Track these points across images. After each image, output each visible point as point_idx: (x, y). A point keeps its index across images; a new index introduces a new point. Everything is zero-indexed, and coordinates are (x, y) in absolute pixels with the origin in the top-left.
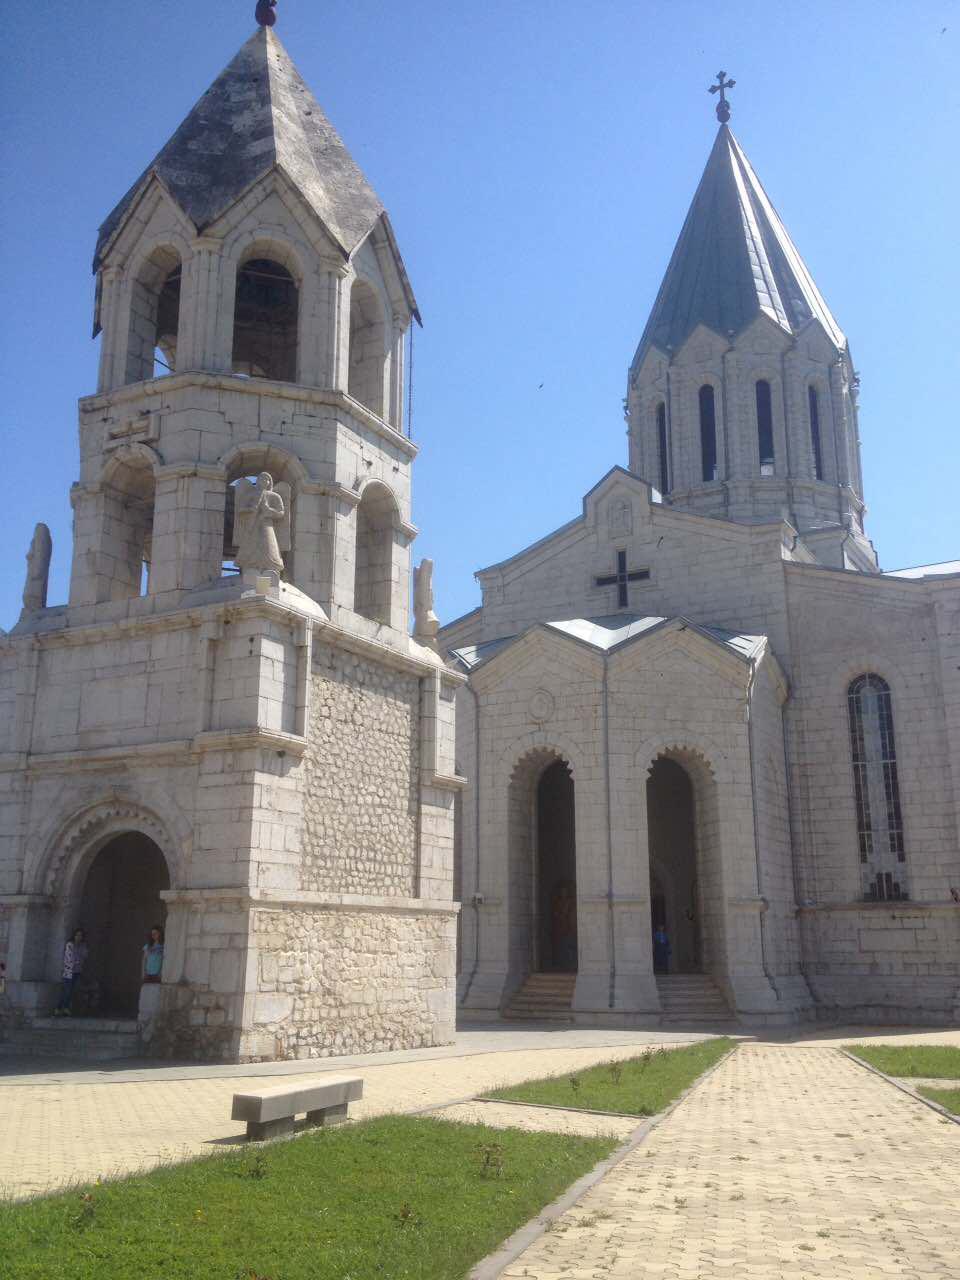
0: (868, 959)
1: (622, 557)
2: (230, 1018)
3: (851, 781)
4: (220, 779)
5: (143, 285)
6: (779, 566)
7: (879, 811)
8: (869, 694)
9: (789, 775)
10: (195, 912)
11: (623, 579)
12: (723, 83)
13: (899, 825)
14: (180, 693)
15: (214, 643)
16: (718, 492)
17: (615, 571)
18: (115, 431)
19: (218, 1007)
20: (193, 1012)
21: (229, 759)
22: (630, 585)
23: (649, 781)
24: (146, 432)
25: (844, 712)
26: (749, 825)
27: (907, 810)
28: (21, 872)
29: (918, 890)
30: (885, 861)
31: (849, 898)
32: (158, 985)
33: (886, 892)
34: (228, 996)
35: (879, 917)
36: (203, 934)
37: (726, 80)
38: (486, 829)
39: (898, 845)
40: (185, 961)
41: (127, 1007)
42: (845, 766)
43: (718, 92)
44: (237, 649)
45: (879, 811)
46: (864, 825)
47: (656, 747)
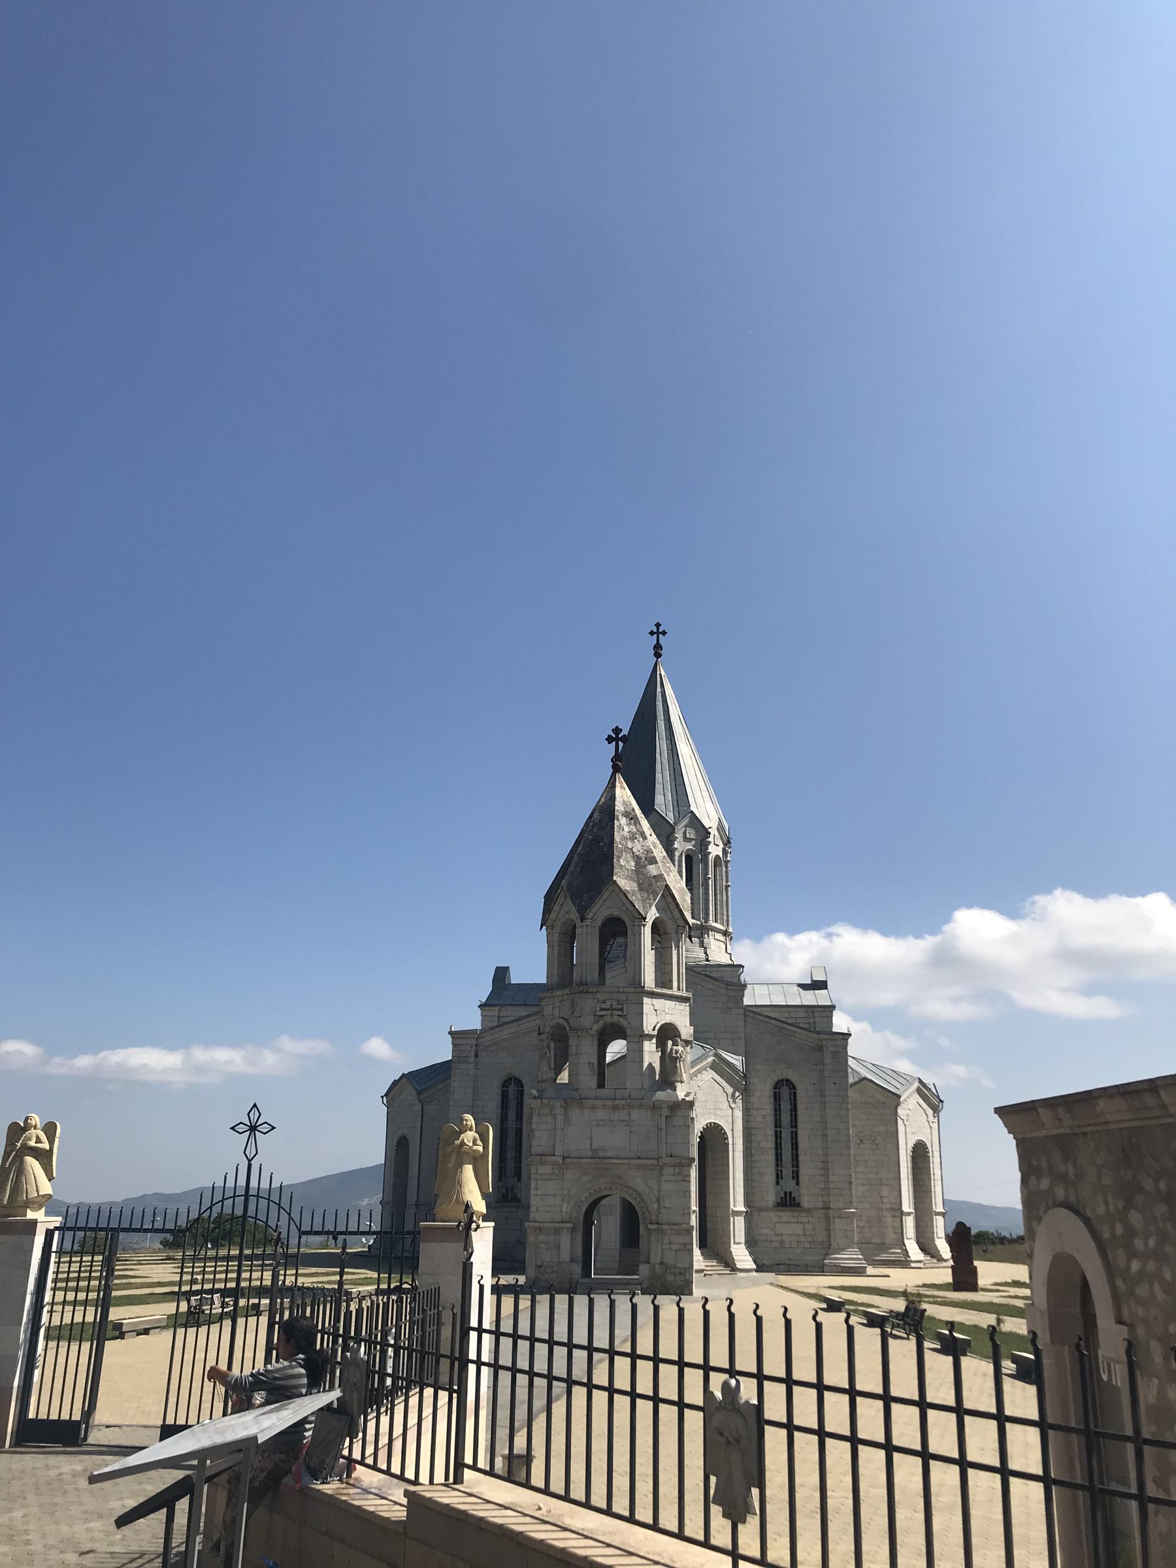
0: (778, 1238)
6: (742, 1011)
8: (785, 1091)
13: (797, 1166)
18: (604, 1006)
21: (677, 1169)
24: (622, 1010)
27: (801, 1158)
29: (805, 1202)
30: (788, 1184)
31: (771, 1205)
33: (788, 1202)
35: (786, 1215)
36: (670, 1243)
39: (796, 1176)
42: (770, 1132)
44: (677, 1121)
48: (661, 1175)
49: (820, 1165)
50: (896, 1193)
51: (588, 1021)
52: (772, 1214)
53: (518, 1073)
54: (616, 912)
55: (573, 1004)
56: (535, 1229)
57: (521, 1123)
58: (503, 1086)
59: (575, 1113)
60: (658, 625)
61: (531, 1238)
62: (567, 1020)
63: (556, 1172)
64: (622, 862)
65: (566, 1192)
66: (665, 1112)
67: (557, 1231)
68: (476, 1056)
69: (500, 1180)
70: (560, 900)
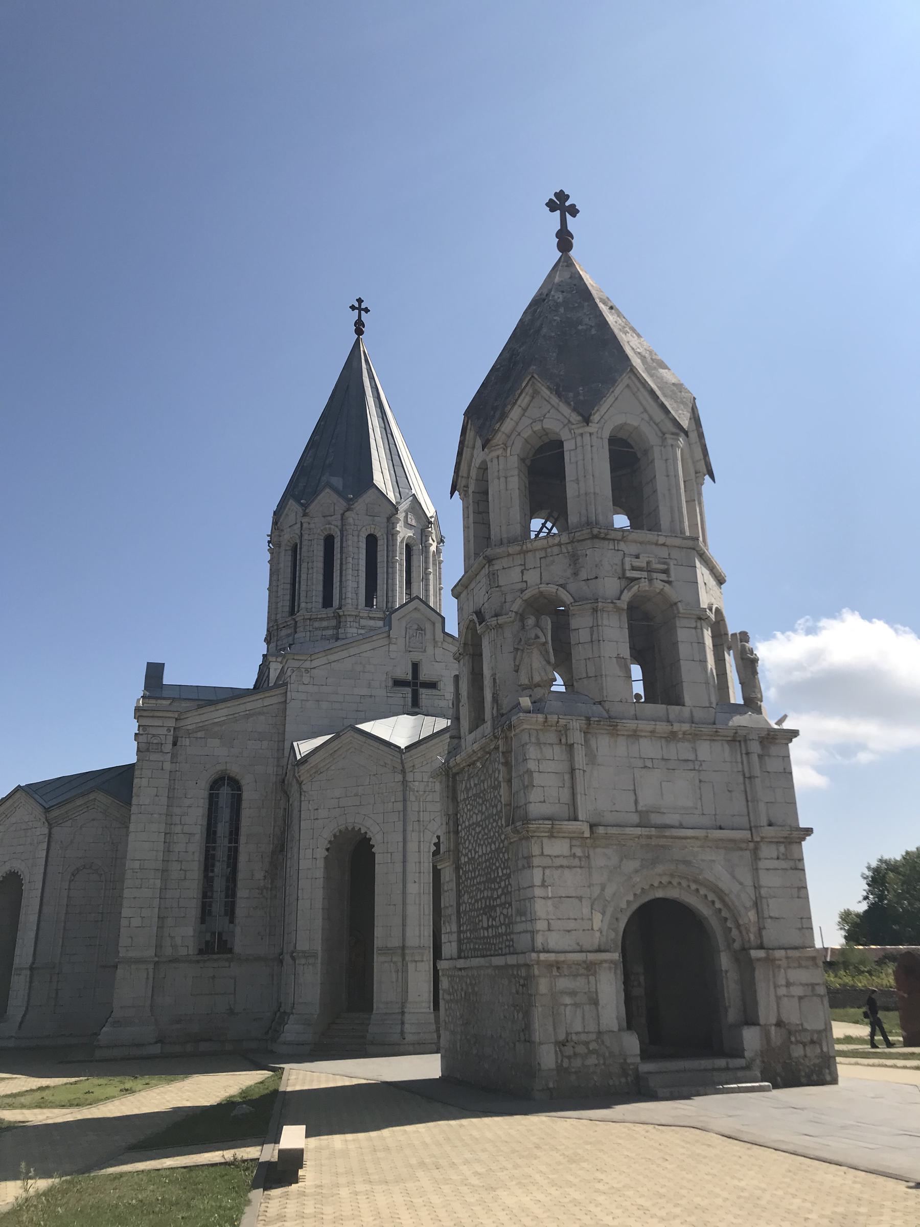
1: (415, 667)
2: (825, 1049)
4: (776, 864)
10: (779, 967)
11: (415, 684)
12: (359, 307)
14: (729, 791)
16: (379, 619)
17: (410, 677)
18: (637, 563)
19: (812, 1042)
20: (793, 1046)
21: (782, 849)
24: (666, 572)
28: (592, 929)
32: (758, 1027)
34: (819, 1032)
36: (788, 985)
37: (363, 306)
40: (778, 1007)
43: (357, 311)
44: (773, 765)
48: (756, 857)
51: (610, 585)
53: (234, 770)
55: (574, 559)
56: (550, 965)
57: (237, 841)
58: (212, 788)
59: (603, 744)
60: (360, 301)
61: (543, 985)
62: (561, 586)
63: (578, 852)
65: (597, 891)
66: (755, 747)
67: (590, 968)
68: (175, 744)
69: (203, 921)
70: (524, 400)
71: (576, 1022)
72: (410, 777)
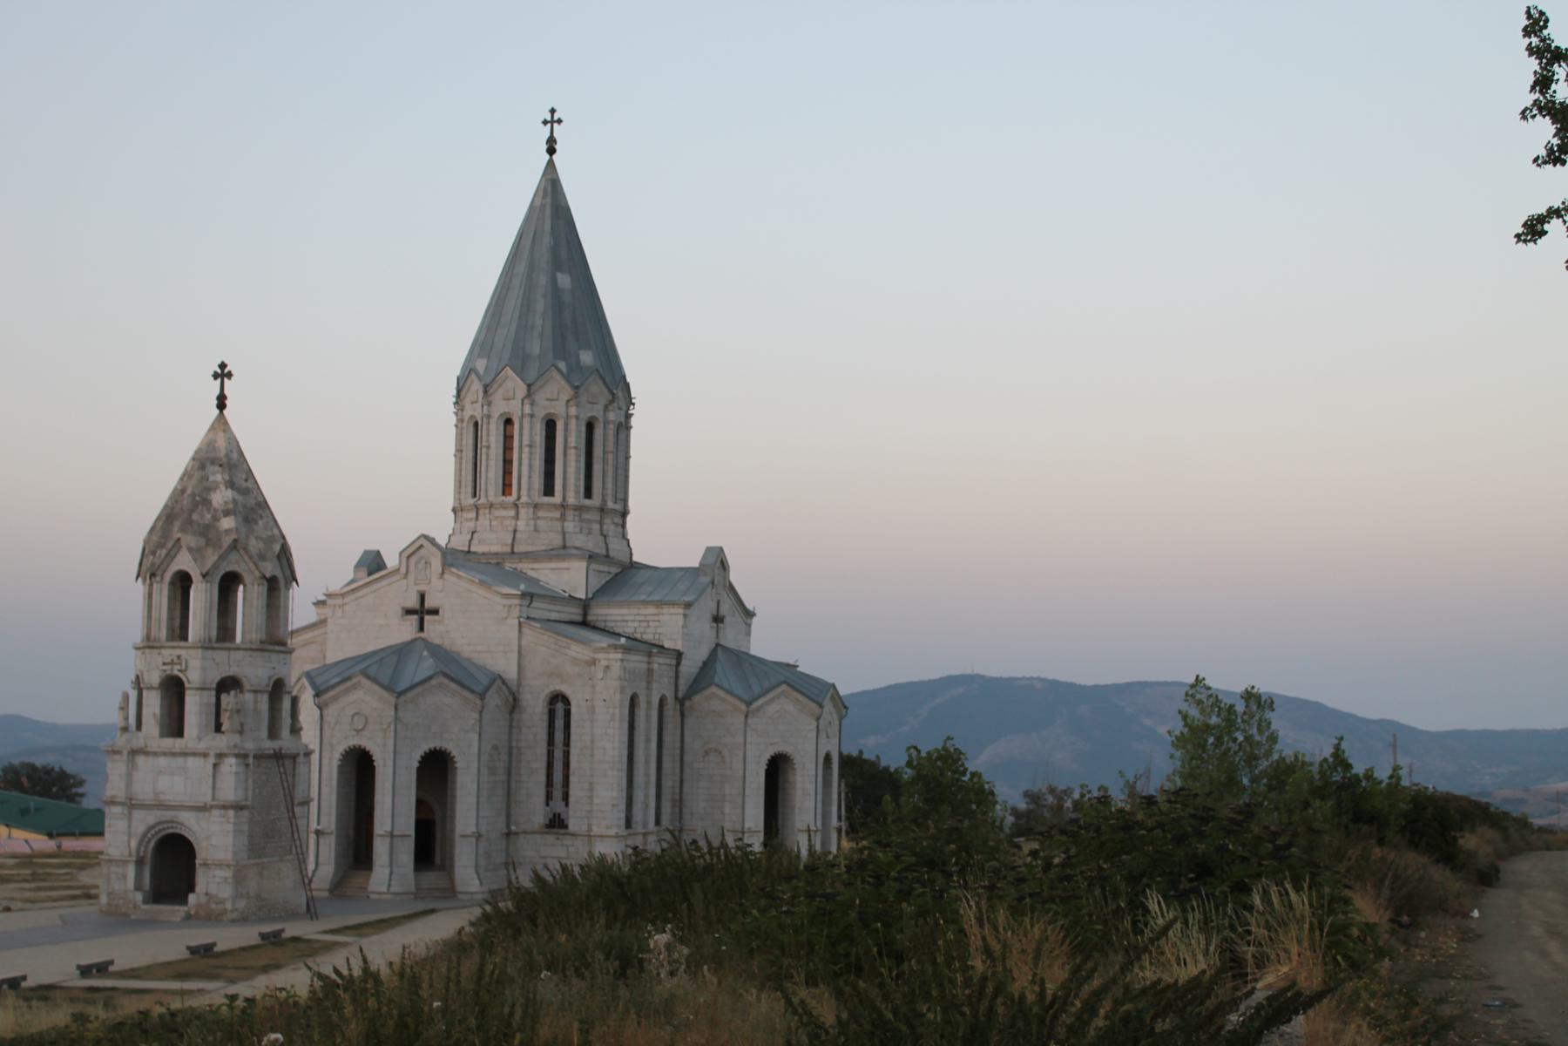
1: (422, 597)
3: (545, 758)
5: (172, 583)
7: (558, 776)
8: (560, 707)
9: (510, 754)
12: (553, 121)
15: (215, 765)
22: (427, 618)
23: (419, 770)
25: (546, 717)
26: (474, 793)
27: (572, 779)
29: (573, 825)
31: (537, 827)
35: (551, 839)
38: (325, 790)
39: (566, 797)
41: (183, 900)
42: (542, 750)
45: (558, 776)
46: (549, 783)
47: (425, 747)
49: (586, 786)
50: (739, 811)
52: (537, 837)
54: (185, 568)
59: (141, 760)
60: (553, 111)
64: (195, 517)
66: (212, 760)
67: (124, 863)
71: (117, 886)
72: (325, 713)
